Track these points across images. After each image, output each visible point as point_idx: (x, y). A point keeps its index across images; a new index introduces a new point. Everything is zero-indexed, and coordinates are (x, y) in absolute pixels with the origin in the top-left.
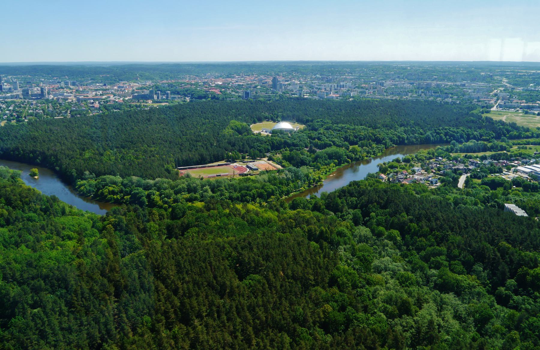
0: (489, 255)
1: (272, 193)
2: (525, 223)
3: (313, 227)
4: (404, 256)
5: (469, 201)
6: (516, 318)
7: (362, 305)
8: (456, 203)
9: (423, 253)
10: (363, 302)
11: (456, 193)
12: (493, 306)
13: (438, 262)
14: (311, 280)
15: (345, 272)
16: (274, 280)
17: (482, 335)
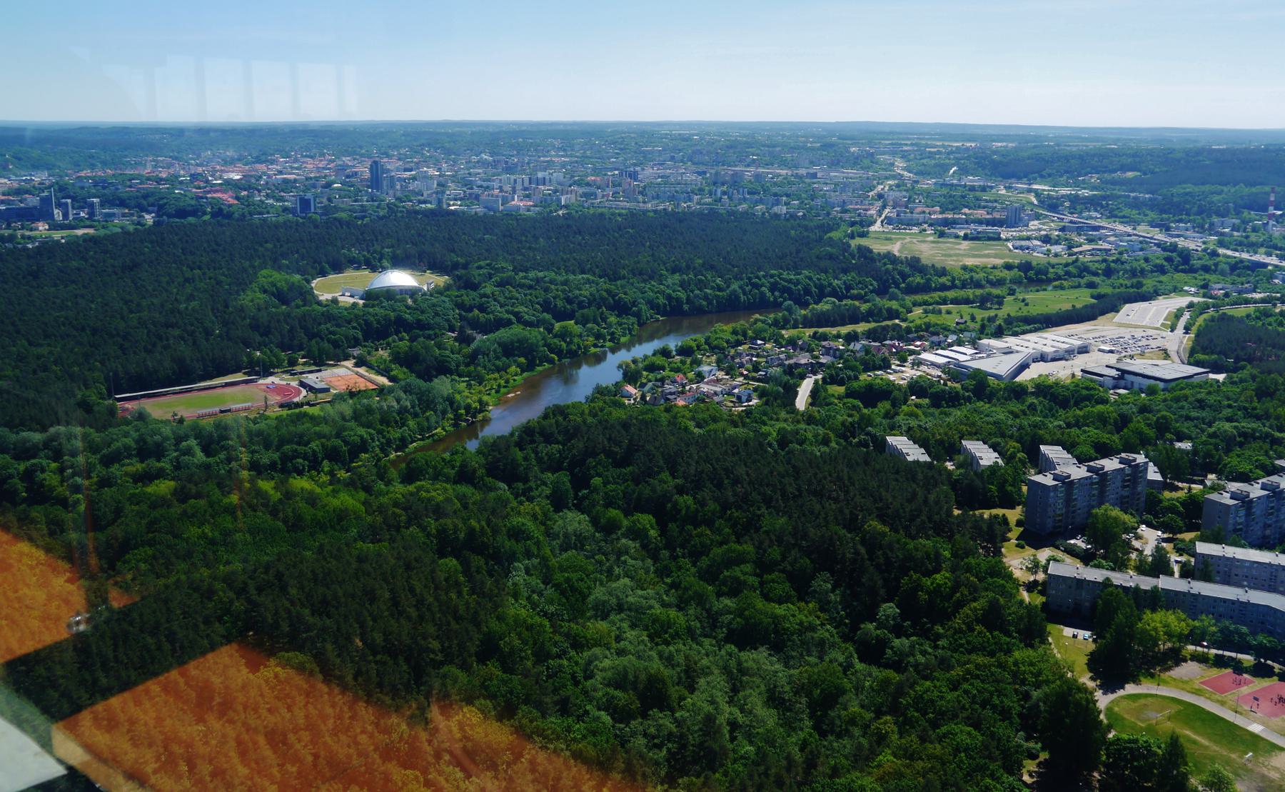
0: (844, 554)
1: (363, 447)
2: (920, 476)
3: (449, 521)
4: (662, 573)
5: (810, 435)
7: (556, 698)
8: (783, 441)
9: (704, 562)
10: (555, 691)
11: (785, 420)
12: (850, 665)
13: (736, 579)
14: (433, 652)
15: (518, 623)
16: (338, 661)
17: (823, 734)
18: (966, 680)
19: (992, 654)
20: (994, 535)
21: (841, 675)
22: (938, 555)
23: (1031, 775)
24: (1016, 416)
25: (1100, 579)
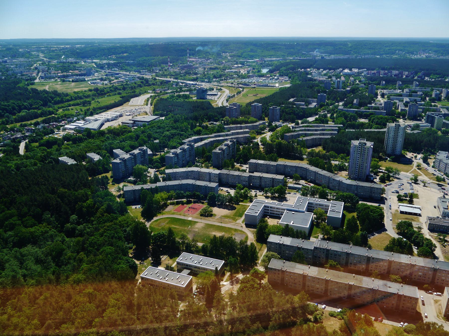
2: (74, 169)
5: (28, 163)
6: (81, 243)
8: (18, 168)
11: (17, 160)
12: (64, 240)
13: (12, 223)
18: (105, 232)
19: (112, 221)
20: (104, 183)
21: (62, 245)
22: (86, 194)
23: (132, 254)
24: (103, 142)
25: (140, 188)
